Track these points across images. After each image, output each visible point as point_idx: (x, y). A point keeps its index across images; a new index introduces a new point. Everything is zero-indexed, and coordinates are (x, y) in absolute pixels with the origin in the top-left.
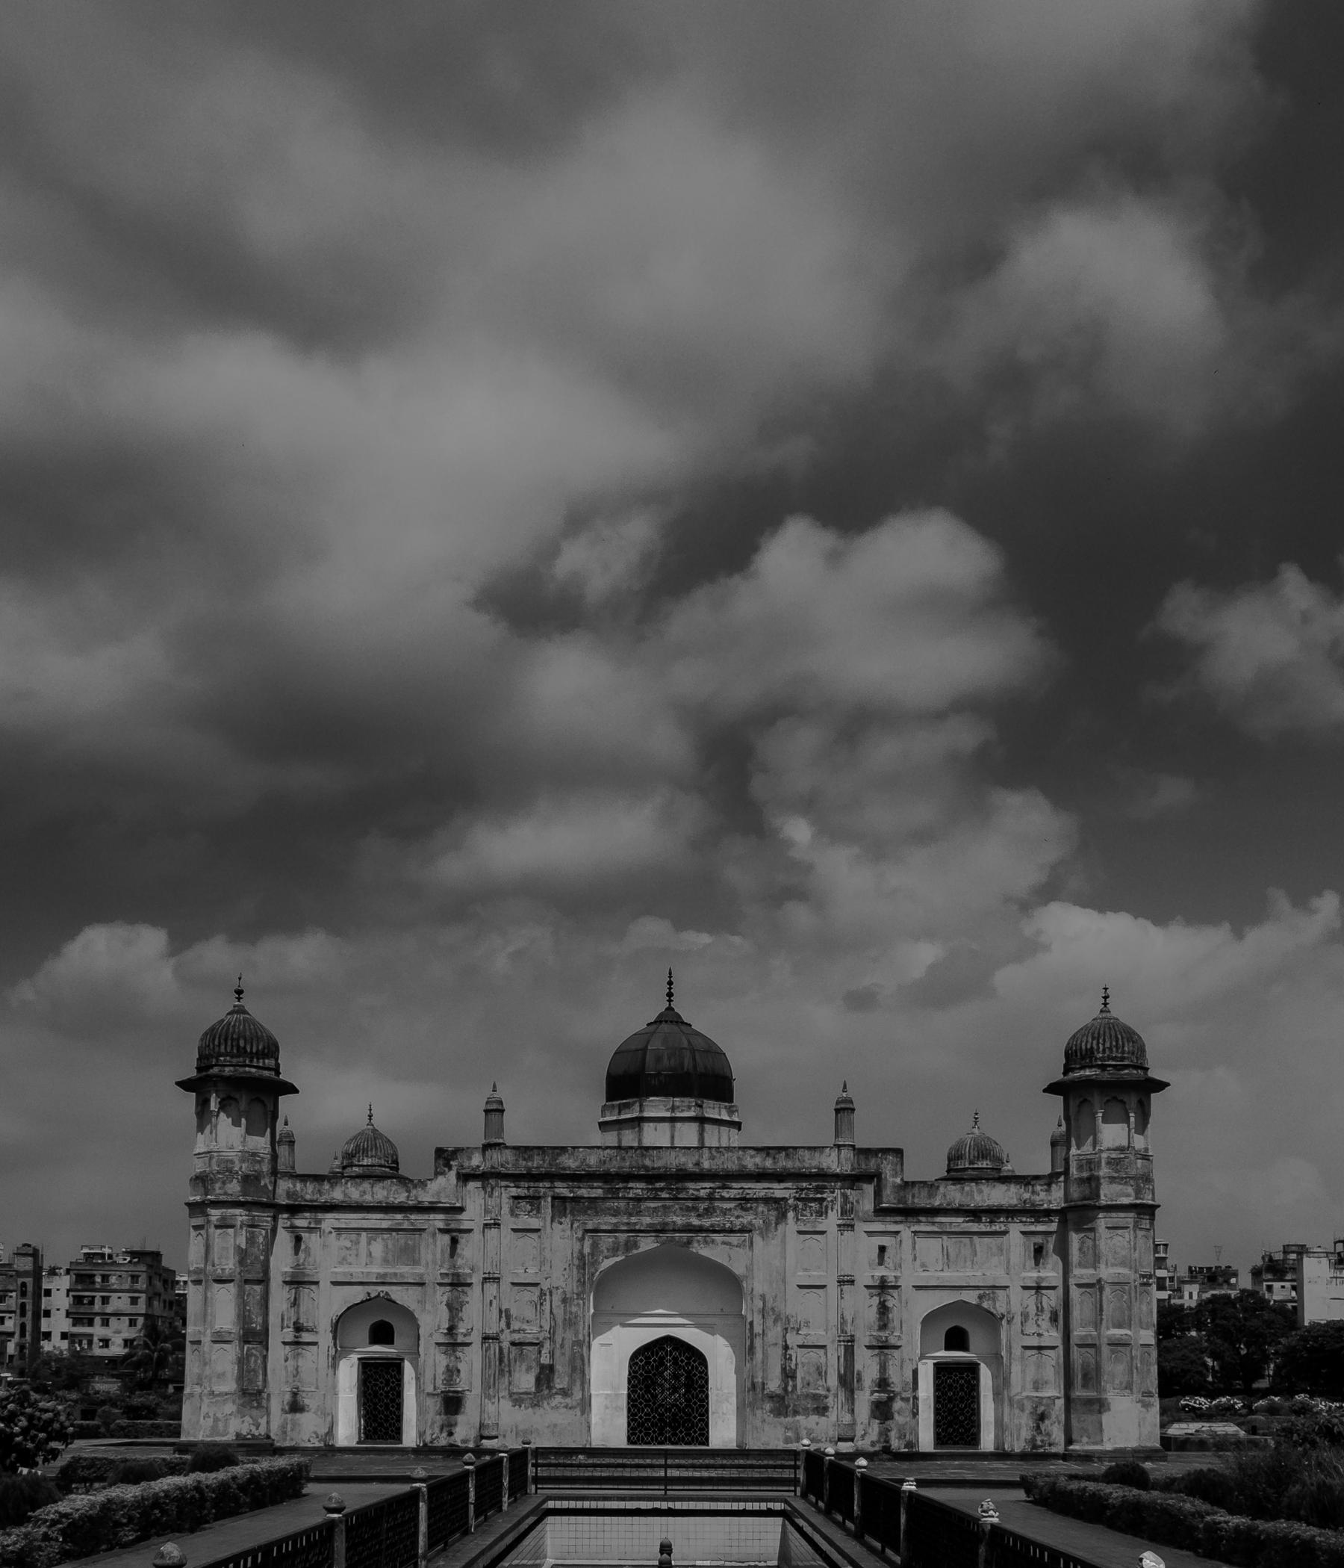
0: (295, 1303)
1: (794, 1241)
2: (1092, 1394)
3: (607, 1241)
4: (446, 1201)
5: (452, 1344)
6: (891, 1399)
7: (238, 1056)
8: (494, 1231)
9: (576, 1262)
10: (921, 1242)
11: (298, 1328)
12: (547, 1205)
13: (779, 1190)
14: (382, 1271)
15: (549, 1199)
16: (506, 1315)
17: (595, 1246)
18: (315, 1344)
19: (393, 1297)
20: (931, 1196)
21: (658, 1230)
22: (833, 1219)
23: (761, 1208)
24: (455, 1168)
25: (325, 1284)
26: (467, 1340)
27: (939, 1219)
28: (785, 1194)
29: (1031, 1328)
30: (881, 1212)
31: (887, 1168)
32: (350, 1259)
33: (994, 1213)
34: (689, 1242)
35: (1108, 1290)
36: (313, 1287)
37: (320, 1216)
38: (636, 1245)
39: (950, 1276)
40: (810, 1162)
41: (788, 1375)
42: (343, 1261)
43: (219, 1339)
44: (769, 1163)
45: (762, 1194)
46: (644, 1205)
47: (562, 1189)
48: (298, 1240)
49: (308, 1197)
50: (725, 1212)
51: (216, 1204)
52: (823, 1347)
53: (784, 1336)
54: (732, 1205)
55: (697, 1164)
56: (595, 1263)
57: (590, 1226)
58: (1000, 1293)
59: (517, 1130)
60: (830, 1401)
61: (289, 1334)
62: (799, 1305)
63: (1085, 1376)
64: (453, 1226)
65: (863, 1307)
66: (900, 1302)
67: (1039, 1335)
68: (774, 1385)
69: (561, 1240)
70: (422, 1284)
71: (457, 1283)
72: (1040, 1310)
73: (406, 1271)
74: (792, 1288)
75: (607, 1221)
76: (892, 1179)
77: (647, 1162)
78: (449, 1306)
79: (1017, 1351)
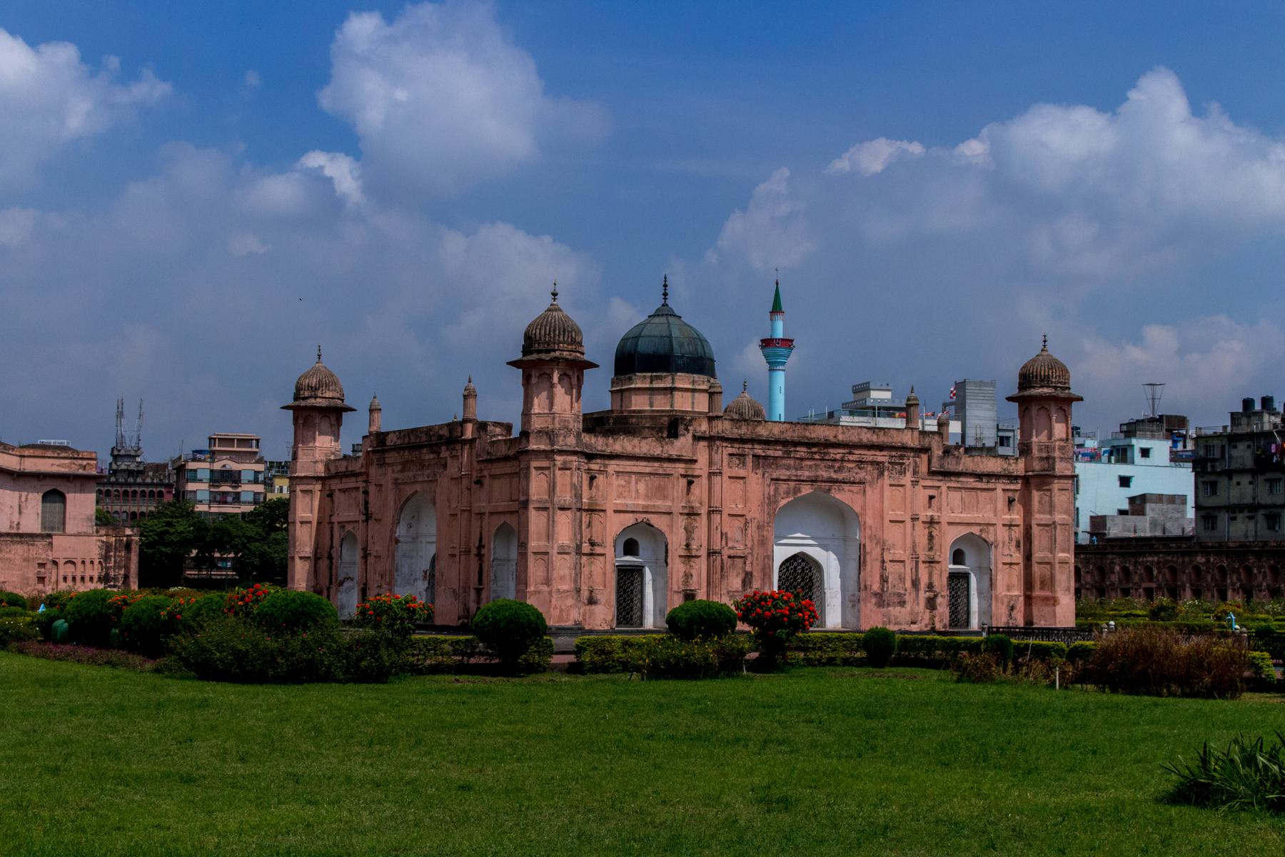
2: (1049, 594)
3: (783, 487)
4: (687, 455)
5: (689, 557)
6: (936, 596)
10: (952, 494)
12: (749, 460)
13: (881, 457)
17: (776, 490)
19: (652, 522)
21: (813, 481)
23: (870, 468)
25: (610, 512)
27: (962, 479)
30: (932, 473)
32: (626, 494)
33: (990, 476)
34: (830, 490)
37: (607, 462)
38: (799, 490)
39: (966, 516)
41: (884, 580)
42: (620, 496)
43: (563, 552)
44: (874, 438)
45: (870, 458)
46: (804, 463)
47: (759, 450)
50: (850, 470)
51: (561, 452)
52: (903, 561)
54: (853, 465)
56: (776, 502)
58: (991, 528)
60: (907, 598)
62: (893, 535)
63: (1042, 583)
65: (921, 533)
69: (757, 484)
71: (692, 514)
72: (1011, 539)
74: (886, 522)
75: (783, 474)
77: (808, 434)
78: (686, 529)
79: (1000, 566)
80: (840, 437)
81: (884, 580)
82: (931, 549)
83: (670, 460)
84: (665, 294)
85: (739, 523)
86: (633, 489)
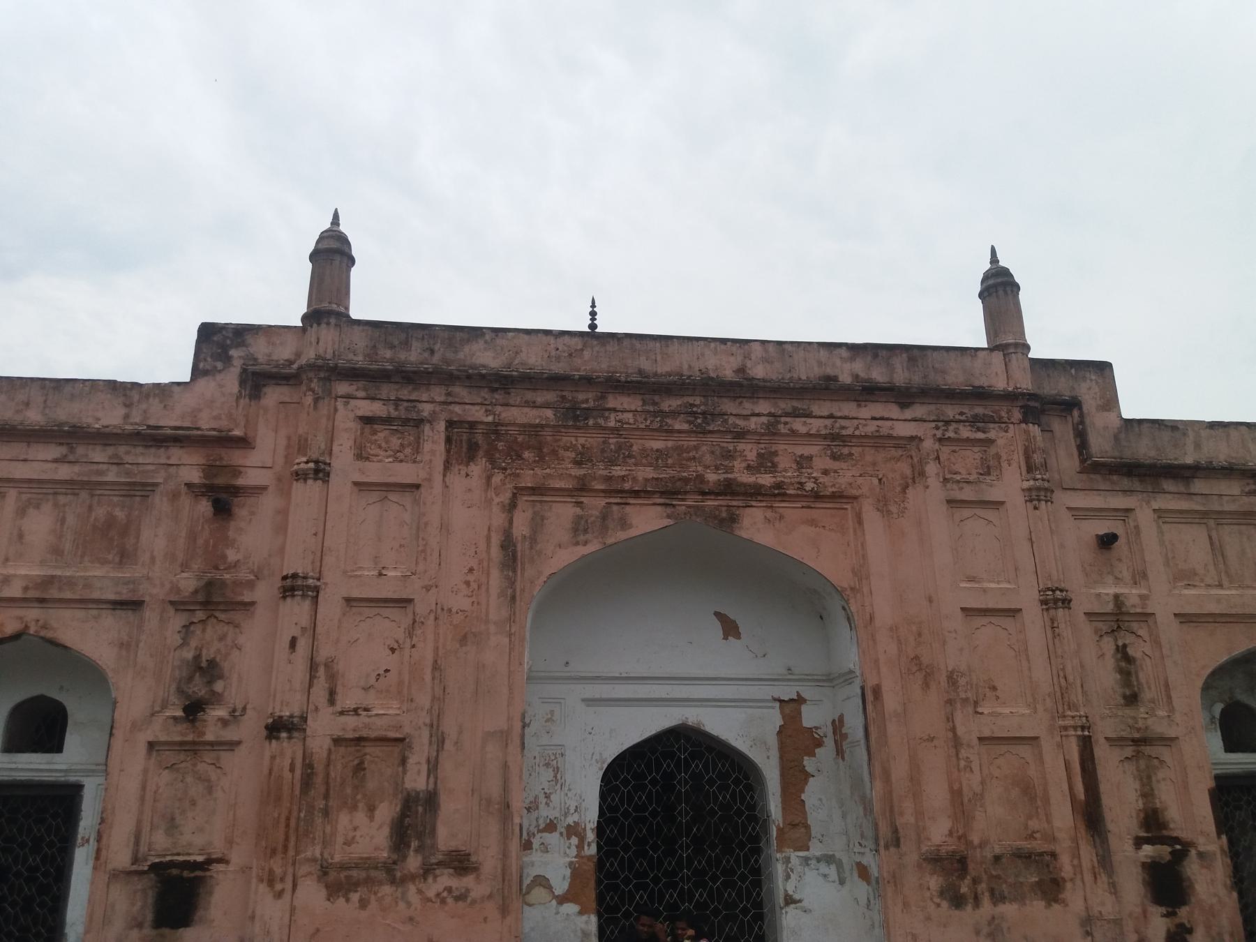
3: (562, 513)
8: (314, 487)
14: (36, 572)
15: (441, 426)
24: (237, 363)
26: (230, 734)
27: (1199, 486)
34: (733, 519)
40: (955, 377)
44: (878, 375)
45: (871, 428)
50: (803, 462)
53: (950, 718)
57: (528, 480)
64: (220, 481)
70: (134, 605)
73: (103, 578)
77: (646, 365)
82: (1132, 699)
85: (390, 626)
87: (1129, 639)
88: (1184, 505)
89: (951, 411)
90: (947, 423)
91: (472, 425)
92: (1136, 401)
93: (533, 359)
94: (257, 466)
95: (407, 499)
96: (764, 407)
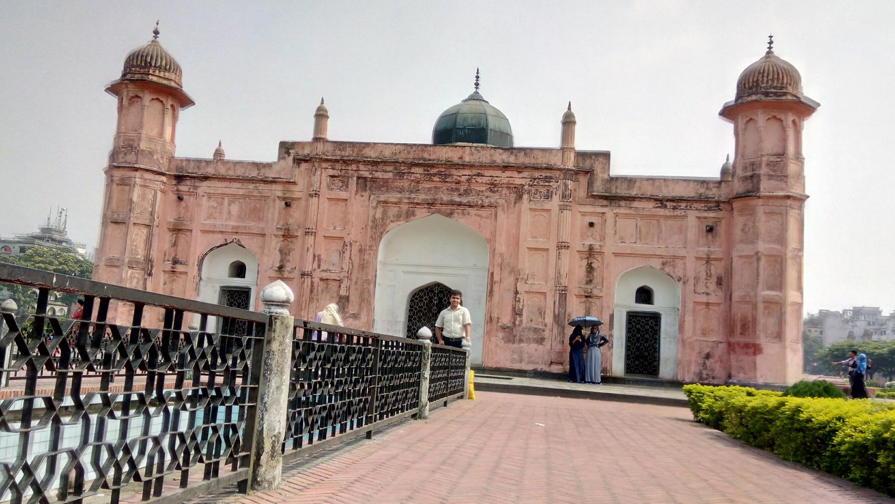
0: (175, 245)
1: (527, 217)
4: (284, 176)
7: (144, 68)
8: (315, 199)
9: (370, 223)
10: (621, 222)
11: (175, 262)
13: (518, 179)
14: (235, 224)
16: (317, 258)
17: (385, 213)
18: (186, 273)
19: (243, 243)
20: (629, 188)
22: (556, 200)
24: (292, 155)
25: (196, 233)
26: (291, 276)
27: (636, 204)
28: (523, 182)
29: (701, 288)
31: (598, 167)
35: (763, 262)
36: (188, 234)
39: (640, 247)
40: (542, 160)
41: (517, 313)
44: (512, 160)
48: (180, 199)
49: (190, 171)
50: (479, 193)
53: (516, 285)
55: (461, 158)
59: (335, 132)
60: (547, 334)
61: (168, 266)
64: (287, 195)
66: (603, 263)
67: (707, 294)
68: (506, 320)
72: (709, 275)
73: (254, 225)
74: (523, 250)
75: (393, 197)
76: (600, 175)
77: (426, 156)
78: (281, 251)
80: (467, 159)
81: (517, 313)
82: (590, 282)
83: (265, 181)
84: (477, 84)
86: (225, 211)
87: (594, 261)
88: (628, 211)
89: (537, 174)
90: (535, 179)
91: (365, 178)
92: (618, 169)
93: (387, 153)
94: (298, 191)
95: (343, 204)
96: (467, 172)
